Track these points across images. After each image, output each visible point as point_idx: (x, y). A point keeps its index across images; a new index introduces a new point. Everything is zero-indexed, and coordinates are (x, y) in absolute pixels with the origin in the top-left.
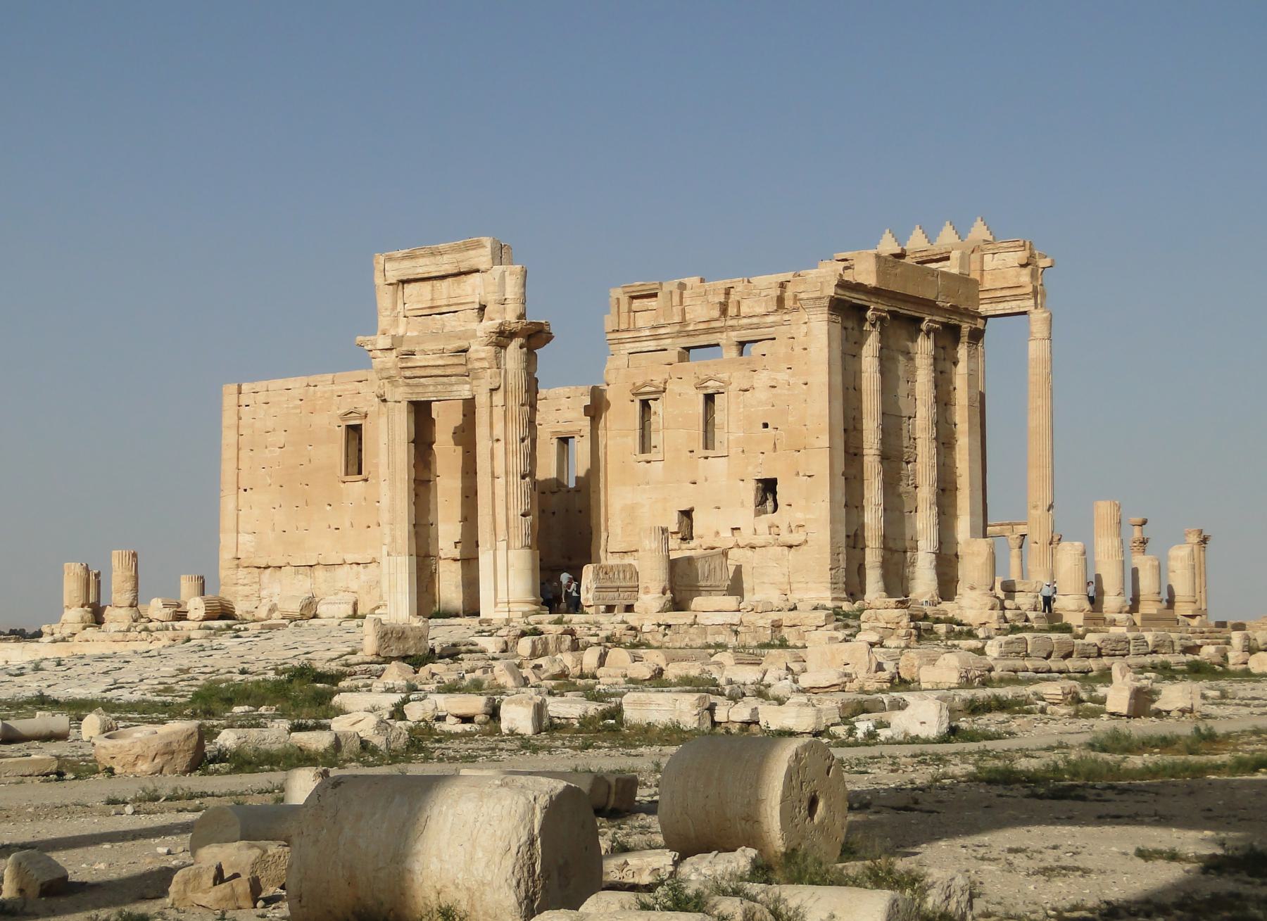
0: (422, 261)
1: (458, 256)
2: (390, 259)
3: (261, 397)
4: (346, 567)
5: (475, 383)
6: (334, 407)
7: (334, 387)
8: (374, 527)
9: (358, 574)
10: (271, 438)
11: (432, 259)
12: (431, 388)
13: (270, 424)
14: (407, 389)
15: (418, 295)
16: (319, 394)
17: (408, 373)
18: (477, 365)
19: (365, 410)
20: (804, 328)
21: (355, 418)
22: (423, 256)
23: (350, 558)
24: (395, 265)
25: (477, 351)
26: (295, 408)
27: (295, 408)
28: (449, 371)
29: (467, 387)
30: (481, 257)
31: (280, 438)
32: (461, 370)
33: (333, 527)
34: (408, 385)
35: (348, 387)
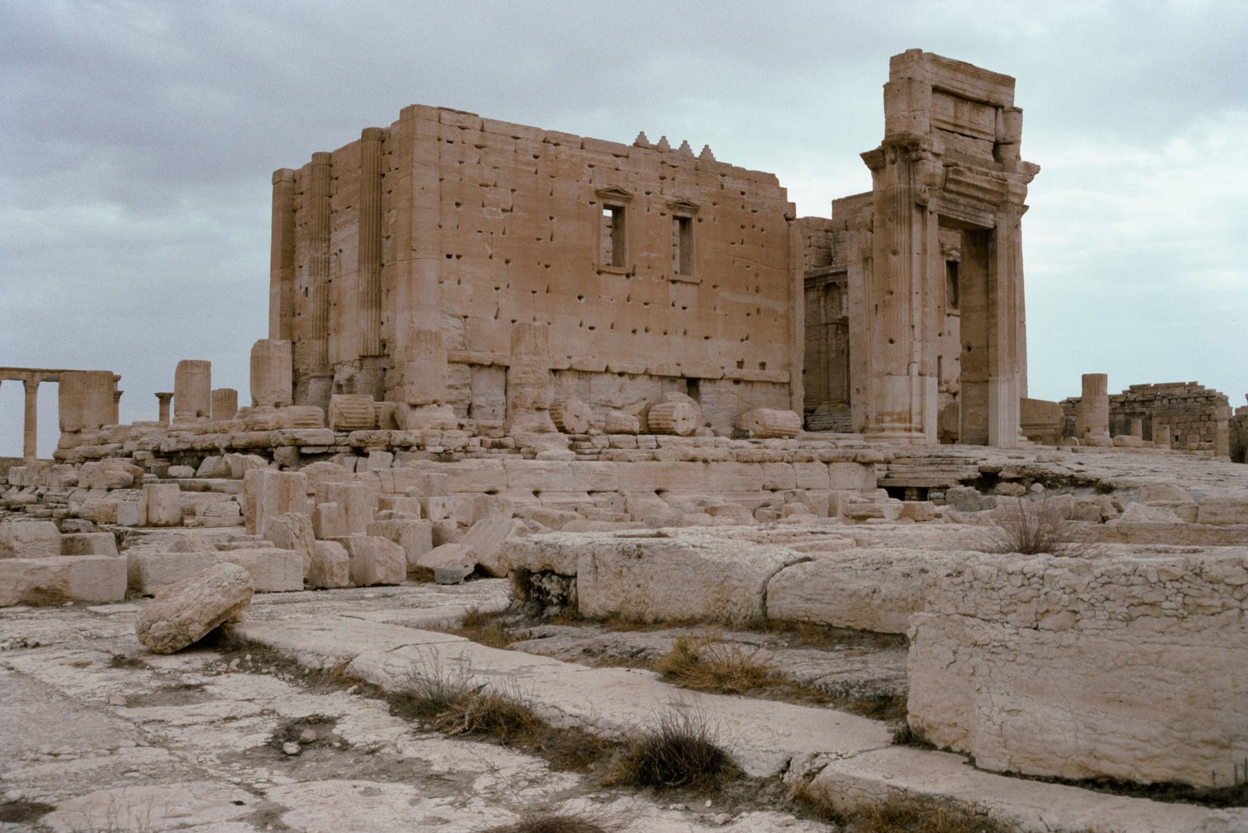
0: (960, 76)
4: (607, 377)
5: (1001, 215)
6: (586, 179)
7: (584, 153)
10: (490, 194)
11: (970, 80)
12: (962, 208)
13: (489, 175)
14: (940, 202)
16: (563, 156)
17: (952, 187)
21: (617, 199)
25: (1016, 186)
26: (528, 164)
27: (528, 164)
28: (987, 197)
29: (991, 216)
31: (509, 200)
33: (587, 324)
34: (943, 198)
35: (601, 157)
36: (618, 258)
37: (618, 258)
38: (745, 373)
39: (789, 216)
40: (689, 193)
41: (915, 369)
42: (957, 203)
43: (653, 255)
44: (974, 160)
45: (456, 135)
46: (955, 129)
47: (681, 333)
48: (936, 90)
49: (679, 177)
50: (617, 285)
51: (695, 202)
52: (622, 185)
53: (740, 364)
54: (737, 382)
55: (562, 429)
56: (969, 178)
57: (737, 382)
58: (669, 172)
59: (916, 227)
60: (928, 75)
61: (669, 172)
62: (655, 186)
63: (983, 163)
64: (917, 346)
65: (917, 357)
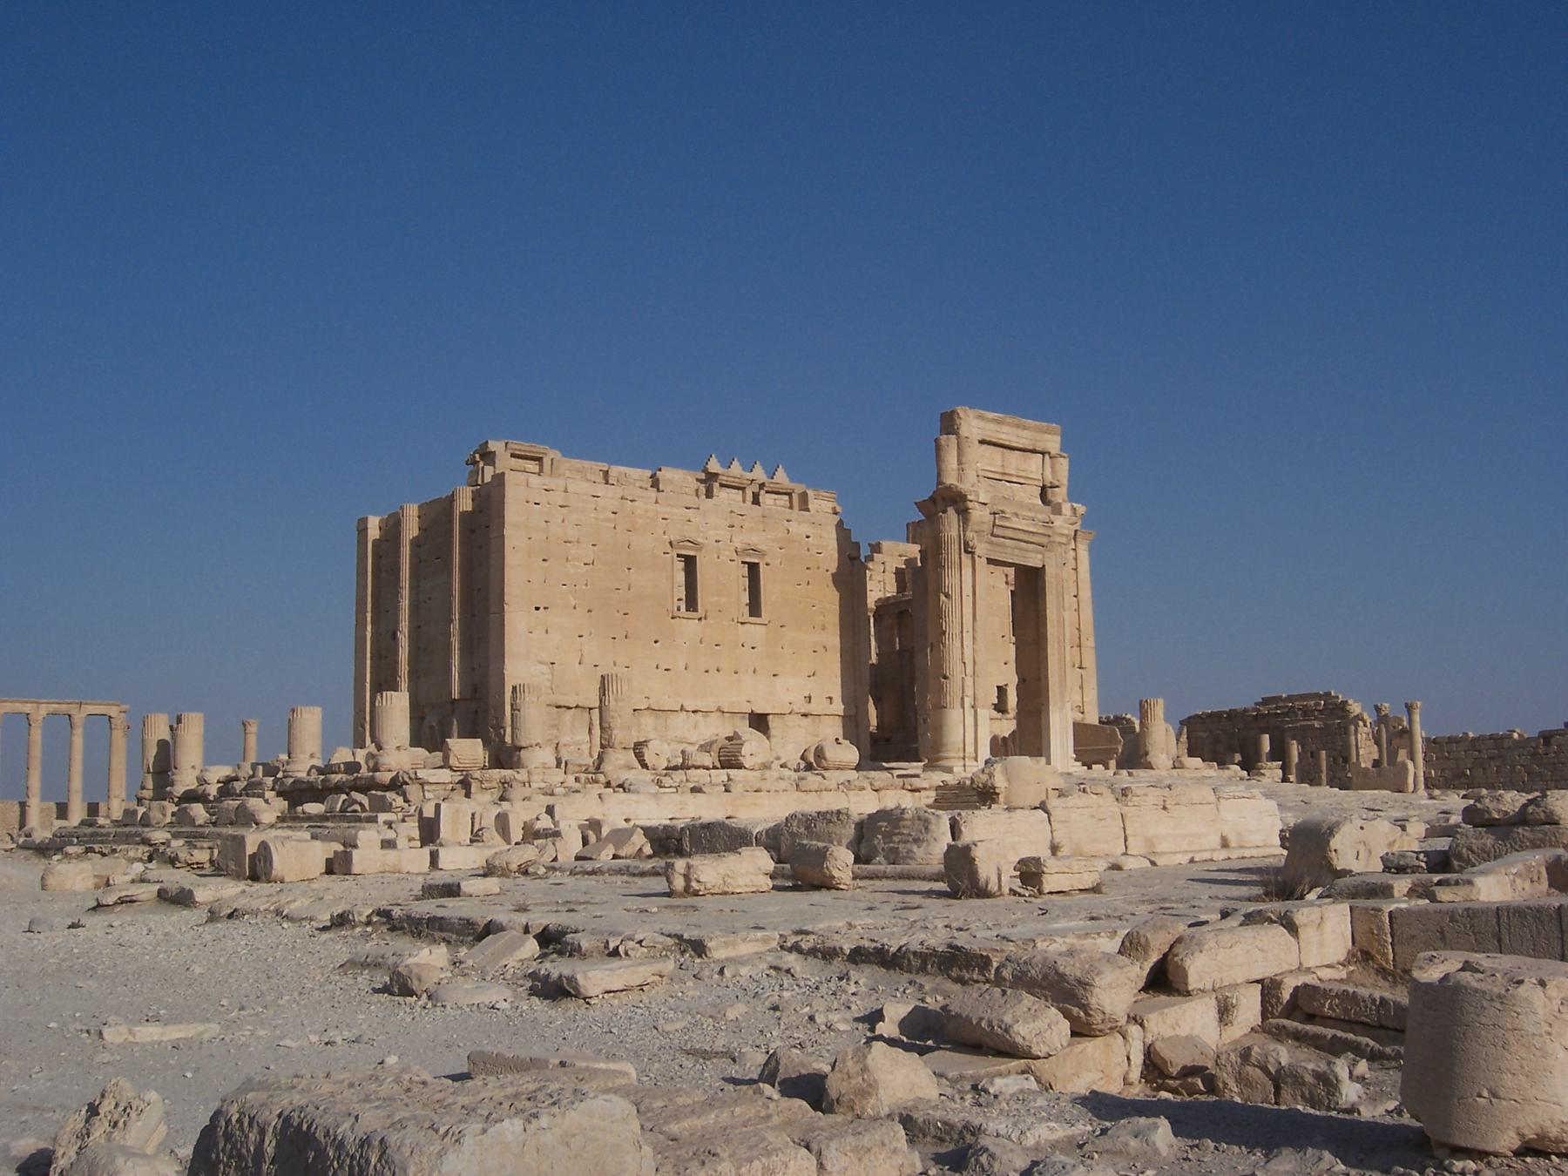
0: (1005, 429)
1: (1038, 436)
2: (980, 417)
3: (558, 498)
8: (713, 671)
9: (696, 727)
10: (573, 550)
13: (572, 533)
15: (991, 460)
18: (1058, 539)
19: (700, 540)
20: (1072, 553)
22: (1009, 424)
23: (690, 706)
24: (981, 424)
26: (608, 520)
27: (608, 520)
30: (1053, 443)
32: (1044, 540)
34: (991, 543)
36: (691, 602)
37: (691, 602)
38: (814, 708)
39: (854, 554)
40: (756, 540)
41: (968, 702)
42: (1005, 546)
43: (723, 600)
44: (1021, 505)
45: (543, 498)
46: (1003, 478)
47: (750, 671)
48: (982, 442)
49: (746, 525)
50: (690, 627)
51: (762, 547)
52: (692, 535)
53: (809, 699)
54: (804, 715)
55: (645, 766)
56: (1015, 523)
57: (804, 715)
58: (737, 521)
59: (967, 571)
60: (975, 430)
61: (737, 521)
62: (724, 534)
63: (1030, 508)
64: (969, 682)
65: (969, 692)
